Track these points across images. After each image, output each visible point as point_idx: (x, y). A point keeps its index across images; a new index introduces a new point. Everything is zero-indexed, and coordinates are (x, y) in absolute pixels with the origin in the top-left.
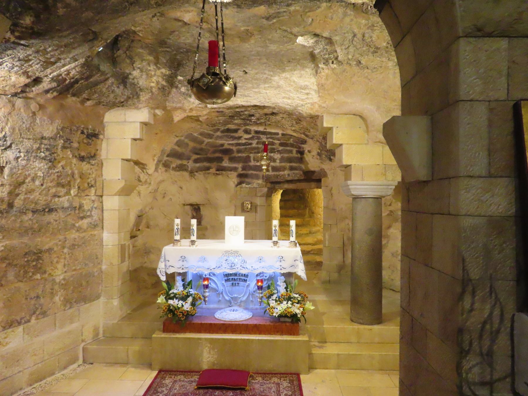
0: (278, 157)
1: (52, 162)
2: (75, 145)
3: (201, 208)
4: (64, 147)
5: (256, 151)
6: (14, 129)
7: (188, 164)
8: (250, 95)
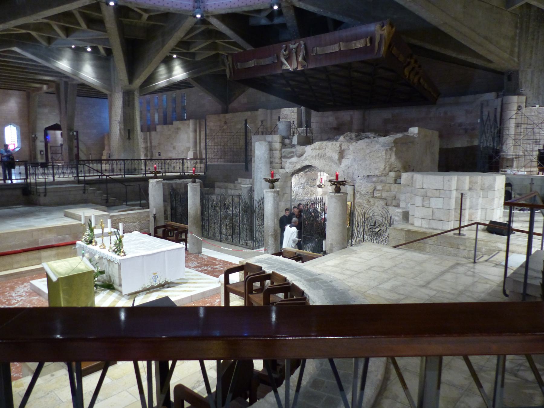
1: (304, 189)
2: (310, 183)
4: (307, 185)
6: (296, 183)
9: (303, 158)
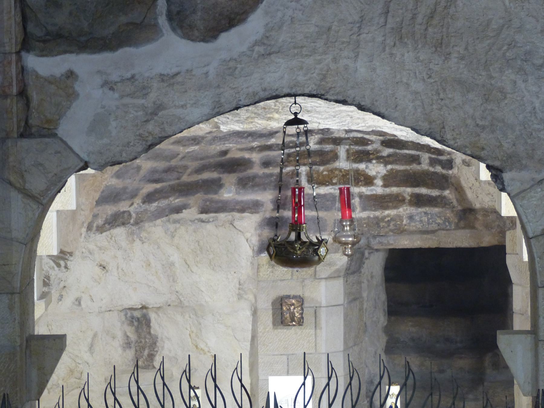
0: (378, 173)
3: (153, 316)
5: (318, 159)
7: (132, 209)
8: (318, 109)
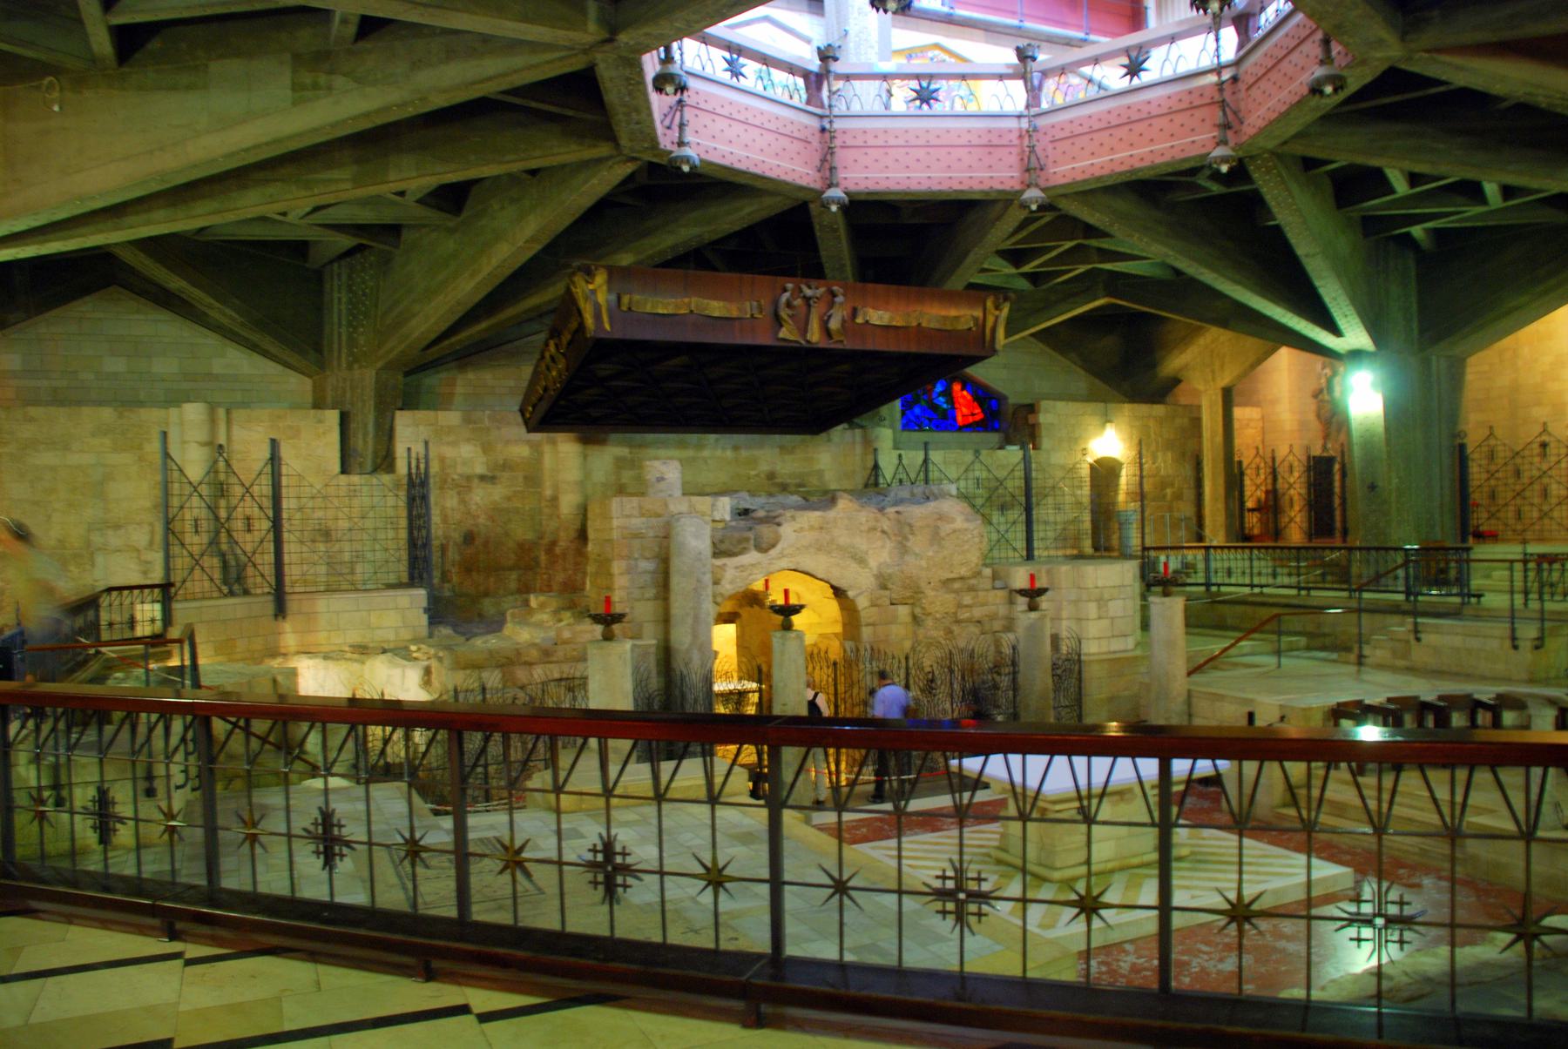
9: (773, 552)
